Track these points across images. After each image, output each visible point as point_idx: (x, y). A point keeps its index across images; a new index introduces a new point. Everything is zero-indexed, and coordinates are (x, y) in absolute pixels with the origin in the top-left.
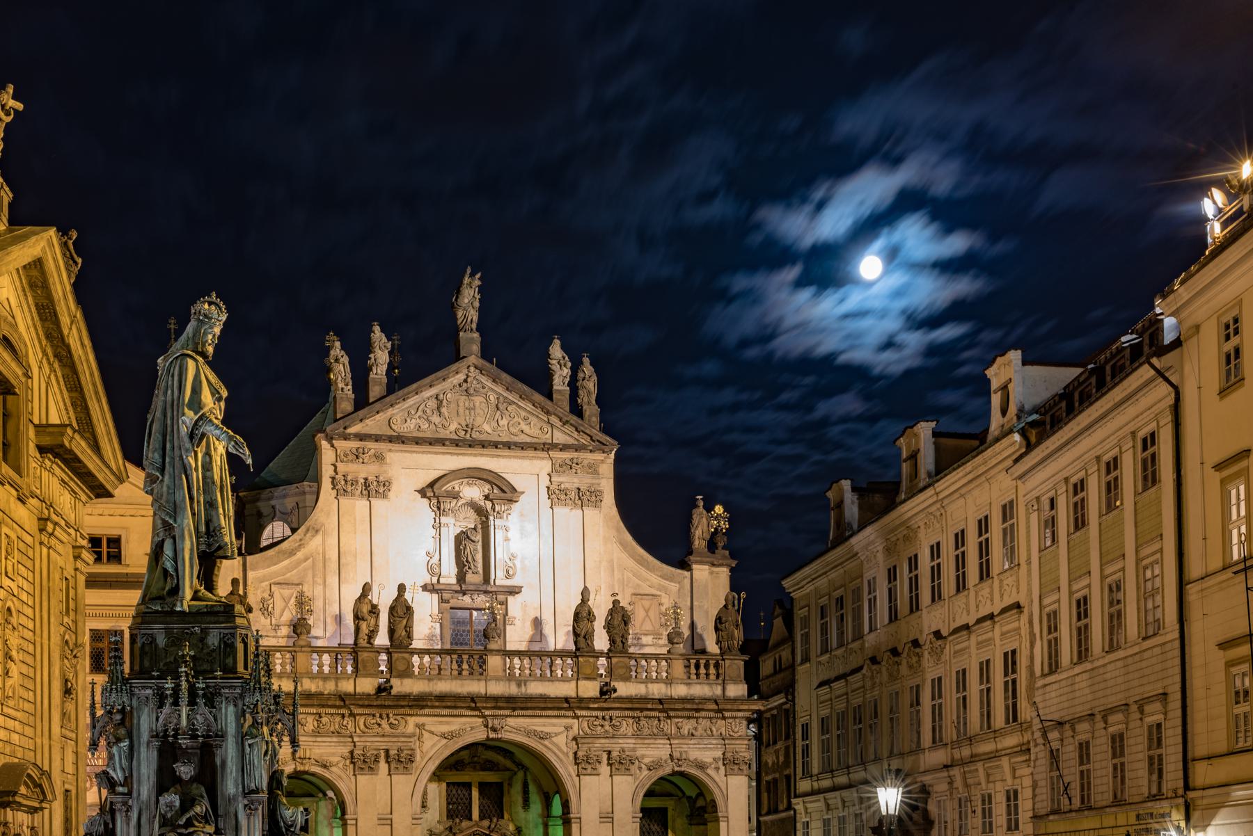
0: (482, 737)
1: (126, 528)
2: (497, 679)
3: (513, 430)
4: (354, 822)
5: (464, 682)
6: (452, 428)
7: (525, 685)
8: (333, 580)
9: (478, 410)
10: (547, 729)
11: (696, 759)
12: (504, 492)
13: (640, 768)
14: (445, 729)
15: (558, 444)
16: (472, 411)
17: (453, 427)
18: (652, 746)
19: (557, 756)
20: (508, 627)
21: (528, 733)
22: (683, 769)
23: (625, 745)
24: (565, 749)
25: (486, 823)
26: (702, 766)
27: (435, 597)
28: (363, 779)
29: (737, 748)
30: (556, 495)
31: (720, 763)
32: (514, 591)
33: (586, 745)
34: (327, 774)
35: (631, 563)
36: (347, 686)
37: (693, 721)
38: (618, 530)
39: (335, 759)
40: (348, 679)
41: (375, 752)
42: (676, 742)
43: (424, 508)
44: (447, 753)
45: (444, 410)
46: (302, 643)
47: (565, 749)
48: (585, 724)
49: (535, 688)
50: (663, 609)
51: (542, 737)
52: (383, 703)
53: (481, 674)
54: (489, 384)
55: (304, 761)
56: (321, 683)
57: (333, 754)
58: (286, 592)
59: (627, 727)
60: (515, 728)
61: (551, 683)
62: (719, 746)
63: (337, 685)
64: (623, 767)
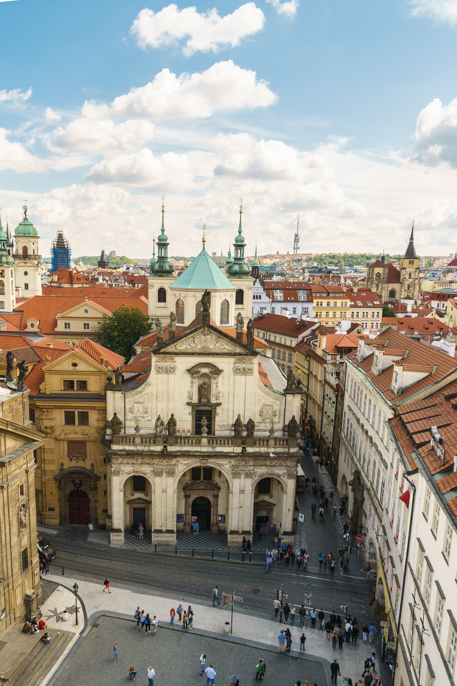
1: (89, 379)
2: (205, 446)
3: (221, 348)
6: (198, 347)
8: (154, 401)
9: (209, 341)
10: (222, 463)
12: (217, 371)
13: (255, 476)
14: (186, 462)
17: (199, 347)
20: (216, 417)
24: (228, 469)
25: (205, 481)
27: (190, 407)
28: (157, 479)
30: (237, 371)
32: (219, 404)
34: (145, 476)
35: (262, 394)
36: (153, 448)
38: (259, 382)
44: (186, 470)
45: (196, 341)
46: (137, 434)
47: (228, 469)
50: (274, 410)
51: (220, 465)
53: (200, 444)
54: (213, 331)
56: (143, 447)
57: (147, 470)
58: (138, 405)
59: (251, 463)
60: (211, 463)
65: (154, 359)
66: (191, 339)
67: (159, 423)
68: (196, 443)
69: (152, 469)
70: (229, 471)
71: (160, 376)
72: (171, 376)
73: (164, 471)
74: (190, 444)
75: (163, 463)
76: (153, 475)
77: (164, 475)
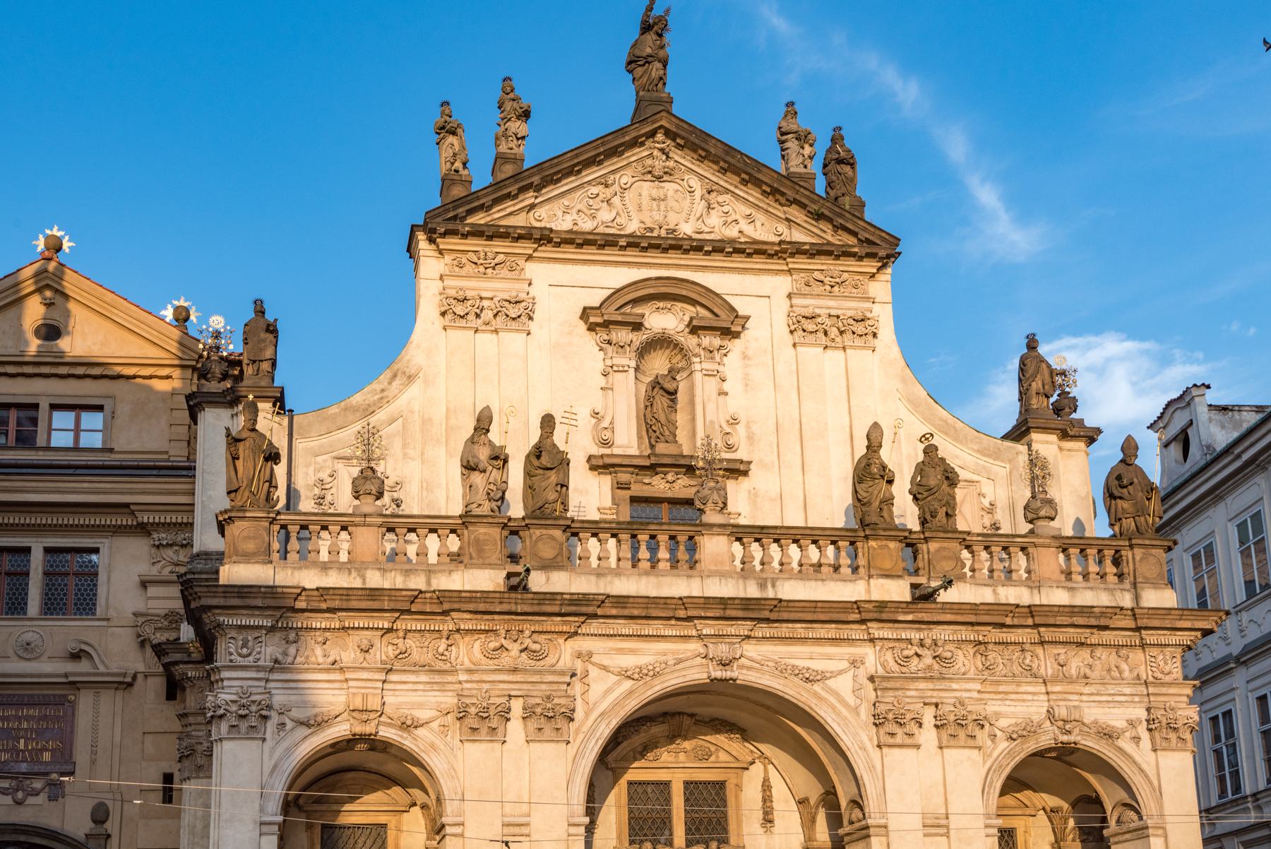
0: (697, 676)
2: (722, 575)
4: (457, 830)
5: (661, 578)
7: (773, 586)
9: (671, 203)
10: (817, 665)
11: (1096, 722)
13: (993, 737)
14: (628, 661)
15: (805, 243)
16: (662, 202)
17: (633, 227)
18: (1013, 696)
19: (839, 714)
21: (782, 670)
22: (1072, 738)
23: (965, 695)
24: (851, 700)
26: (1109, 735)
28: (477, 752)
29: (1172, 702)
31: (1142, 731)
33: (891, 693)
34: (407, 742)
37: (1085, 653)
39: (423, 715)
40: (450, 572)
41: (499, 701)
42: (1058, 688)
43: (588, 343)
44: (632, 705)
45: (616, 200)
46: (367, 509)
47: (851, 700)
48: (889, 656)
49: (792, 590)
51: (810, 679)
52: (513, 608)
53: (691, 568)
55: (365, 717)
57: (421, 706)
59: (965, 660)
61: (820, 583)
62: (1137, 699)
63: (429, 583)
64: (962, 734)
65: (431, 265)
66: (595, 190)
67: (483, 454)
68: (674, 563)
69: (450, 700)
70: (856, 710)
71: (460, 337)
72: (513, 340)
73: (517, 707)
74: (645, 565)
75: (506, 660)
76: (454, 737)
77: (515, 728)
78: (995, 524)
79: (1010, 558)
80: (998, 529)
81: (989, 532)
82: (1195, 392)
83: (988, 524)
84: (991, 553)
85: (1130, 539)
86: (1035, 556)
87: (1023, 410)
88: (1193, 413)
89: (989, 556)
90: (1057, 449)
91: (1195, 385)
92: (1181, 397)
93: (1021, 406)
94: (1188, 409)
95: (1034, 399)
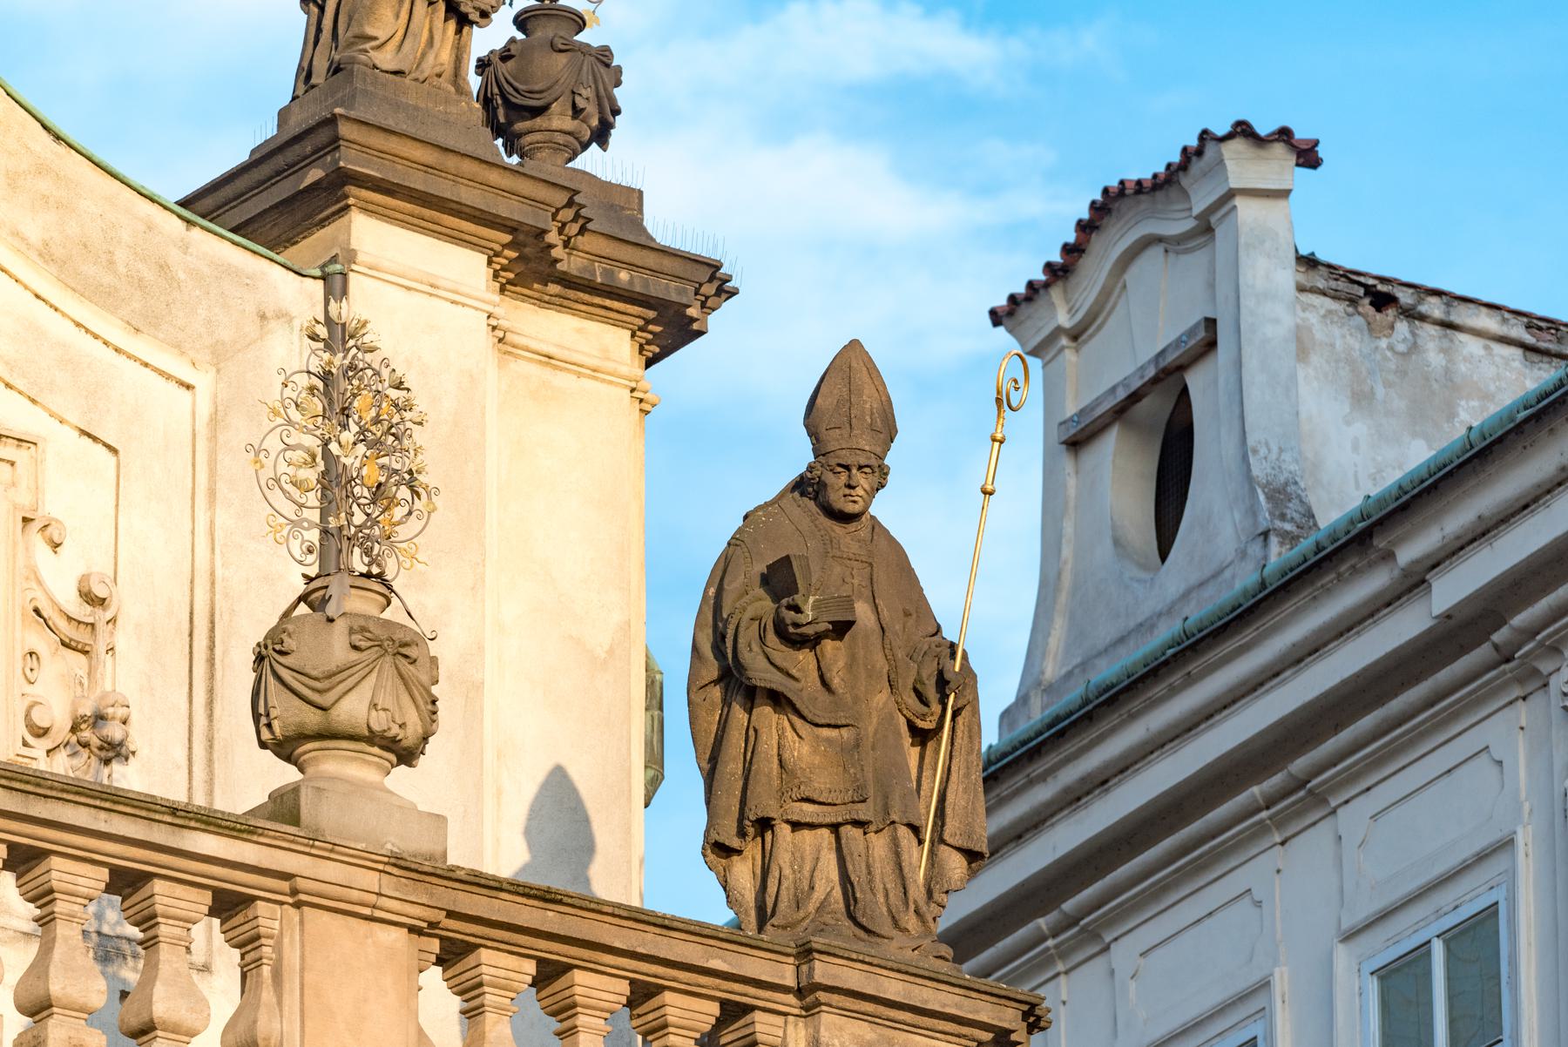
78: (99, 718)
79: (150, 943)
80: (113, 751)
81: (61, 765)
82: (1241, 166)
83: (58, 717)
84: (42, 897)
85: (805, 953)
86: (292, 957)
87: (321, 65)
88: (1223, 289)
89: (32, 910)
90: (484, 338)
91: (1243, 130)
92: (1168, 182)
93: (314, 37)
94: (1194, 263)
95: (386, 13)
